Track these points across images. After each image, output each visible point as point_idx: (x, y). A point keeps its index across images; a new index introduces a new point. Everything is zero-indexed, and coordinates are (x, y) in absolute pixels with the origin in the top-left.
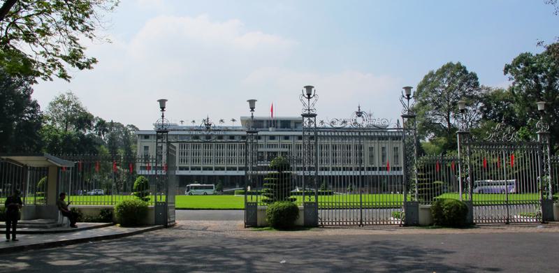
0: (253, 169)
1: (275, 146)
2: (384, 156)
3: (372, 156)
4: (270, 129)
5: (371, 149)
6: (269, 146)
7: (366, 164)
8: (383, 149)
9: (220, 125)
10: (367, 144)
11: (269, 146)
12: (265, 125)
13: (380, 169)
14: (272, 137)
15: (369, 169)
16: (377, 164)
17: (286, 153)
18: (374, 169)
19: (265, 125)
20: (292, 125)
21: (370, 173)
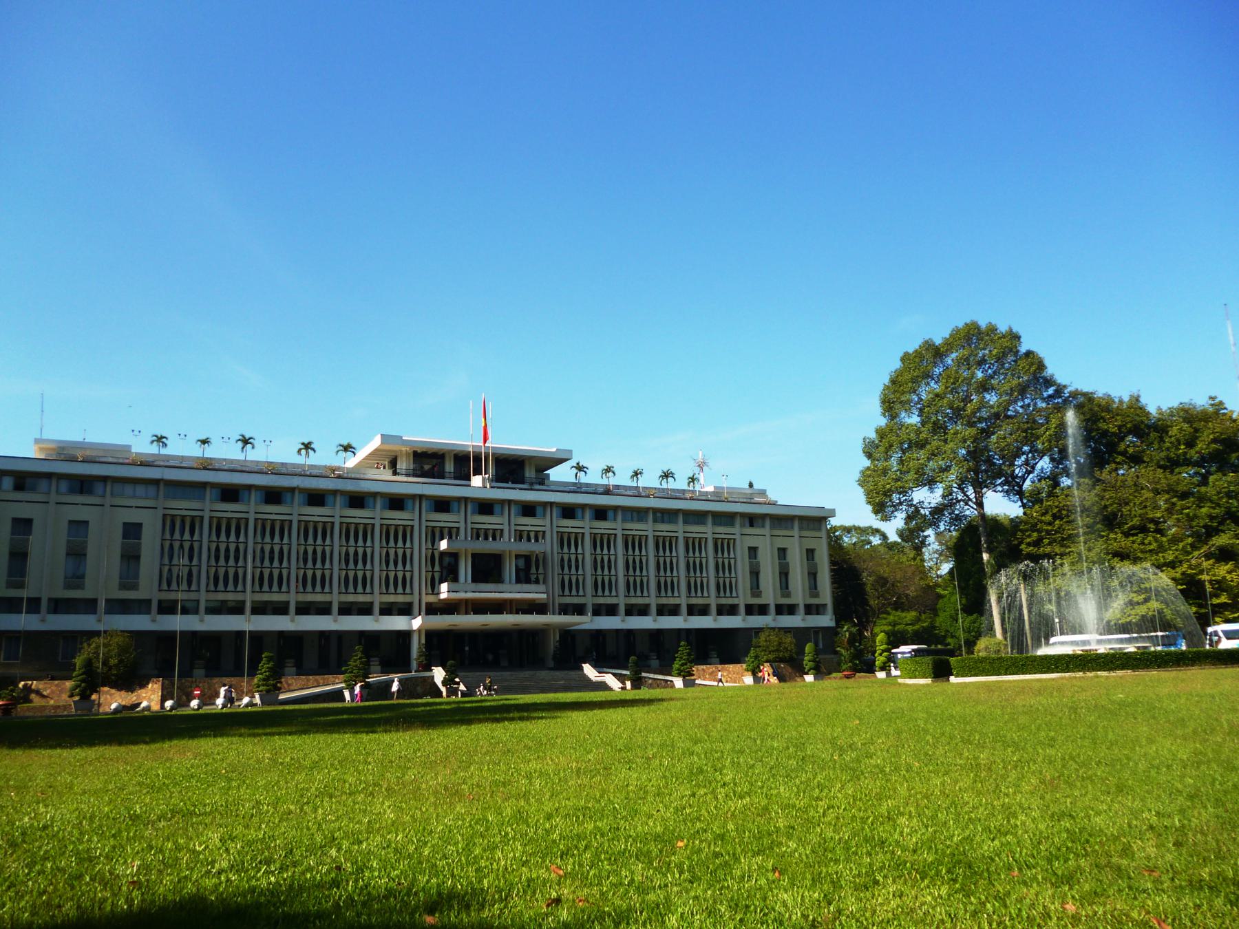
0: (431, 610)
1: (496, 535)
2: (784, 574)
3: (755, 574)
4: (476, 481)
5: (753, 551)
6: (477, 534)
7: (743, 597)
8: (782, 552)
9: (300, 460)
10: (744, 538)
11: (477, 534)
12: (449, 467)
13: (780, 610)
14: (486, 507)
15: (750, 610)
16: (769, 595)
17: (527, 558)
18: (763, 610)
19: (449, 467)
20: (529, 473)
21: (756, 621)
